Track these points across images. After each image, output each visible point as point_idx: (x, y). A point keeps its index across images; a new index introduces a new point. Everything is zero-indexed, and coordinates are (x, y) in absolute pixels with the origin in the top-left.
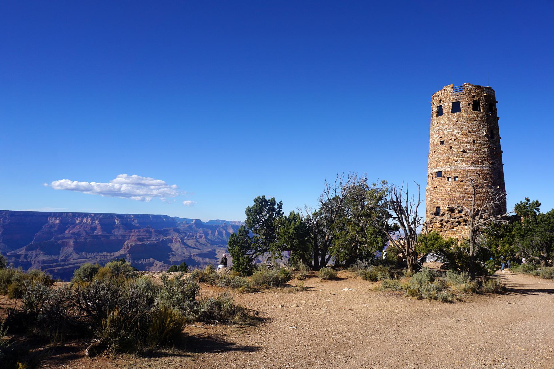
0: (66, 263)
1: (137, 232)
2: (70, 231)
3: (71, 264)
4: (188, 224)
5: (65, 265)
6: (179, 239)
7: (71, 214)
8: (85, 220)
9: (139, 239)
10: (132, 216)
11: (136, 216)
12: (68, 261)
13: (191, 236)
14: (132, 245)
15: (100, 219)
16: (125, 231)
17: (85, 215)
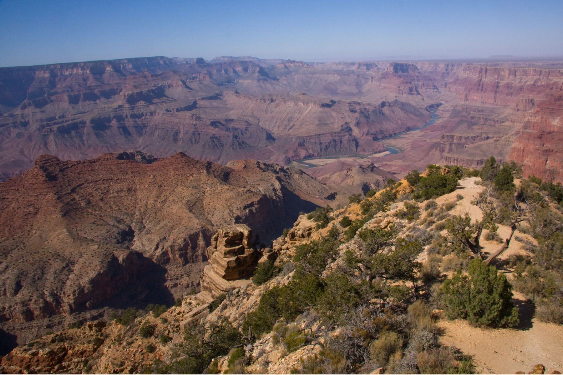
0: (64, 120)
1: (133, 79)
2: (62, 84)
3: (68, 121)
4: (190, 64)
5: (63, 122)
6: (180, 83)
7: (59, 65)
8: (75, 71)
9: (136, 87)
10: (126, 61)
11: (130, 60)
12: (66, 117)
13: (193, 78)
14: (128, 94)
15: (91, 68)
16: (120, 79)
17: (75, 65)
